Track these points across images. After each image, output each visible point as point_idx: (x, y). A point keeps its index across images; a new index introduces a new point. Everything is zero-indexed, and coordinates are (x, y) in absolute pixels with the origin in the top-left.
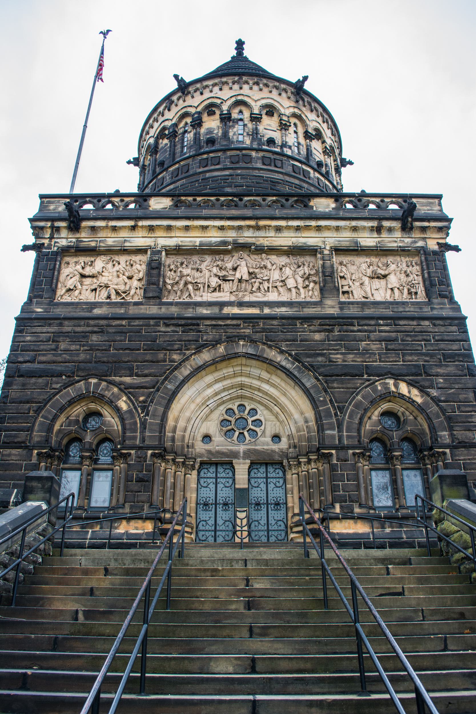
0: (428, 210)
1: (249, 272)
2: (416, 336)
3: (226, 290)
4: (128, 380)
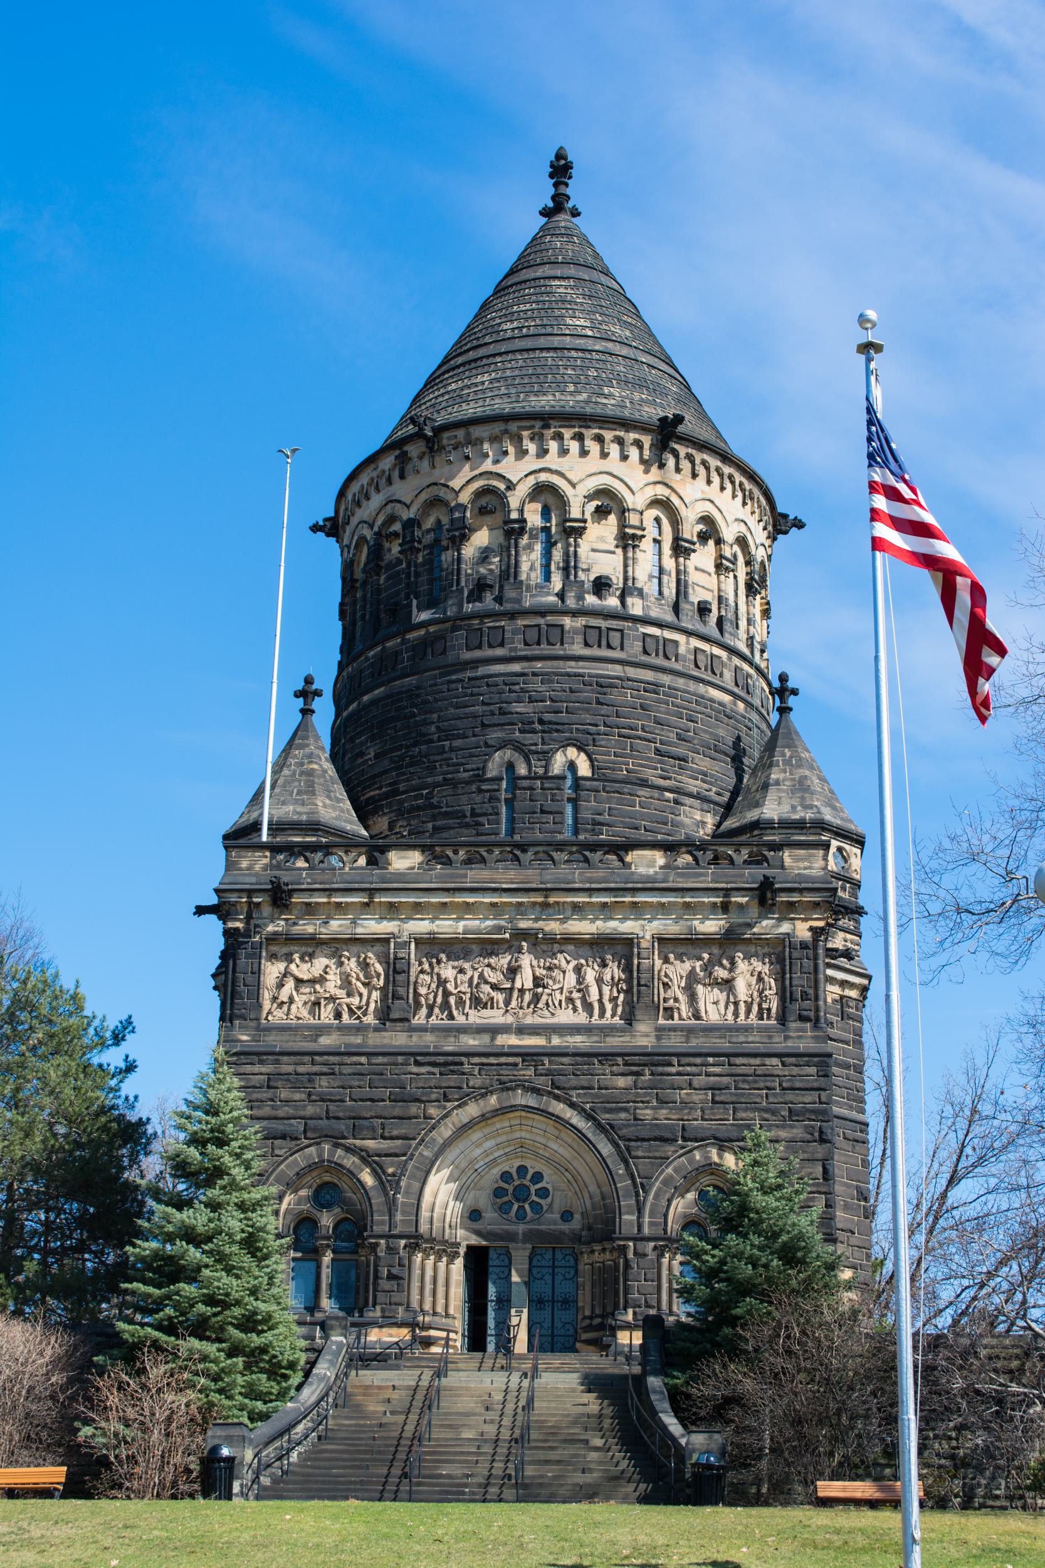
0: (805, 868)
2: (755, 1082)
4: (370, 1144)
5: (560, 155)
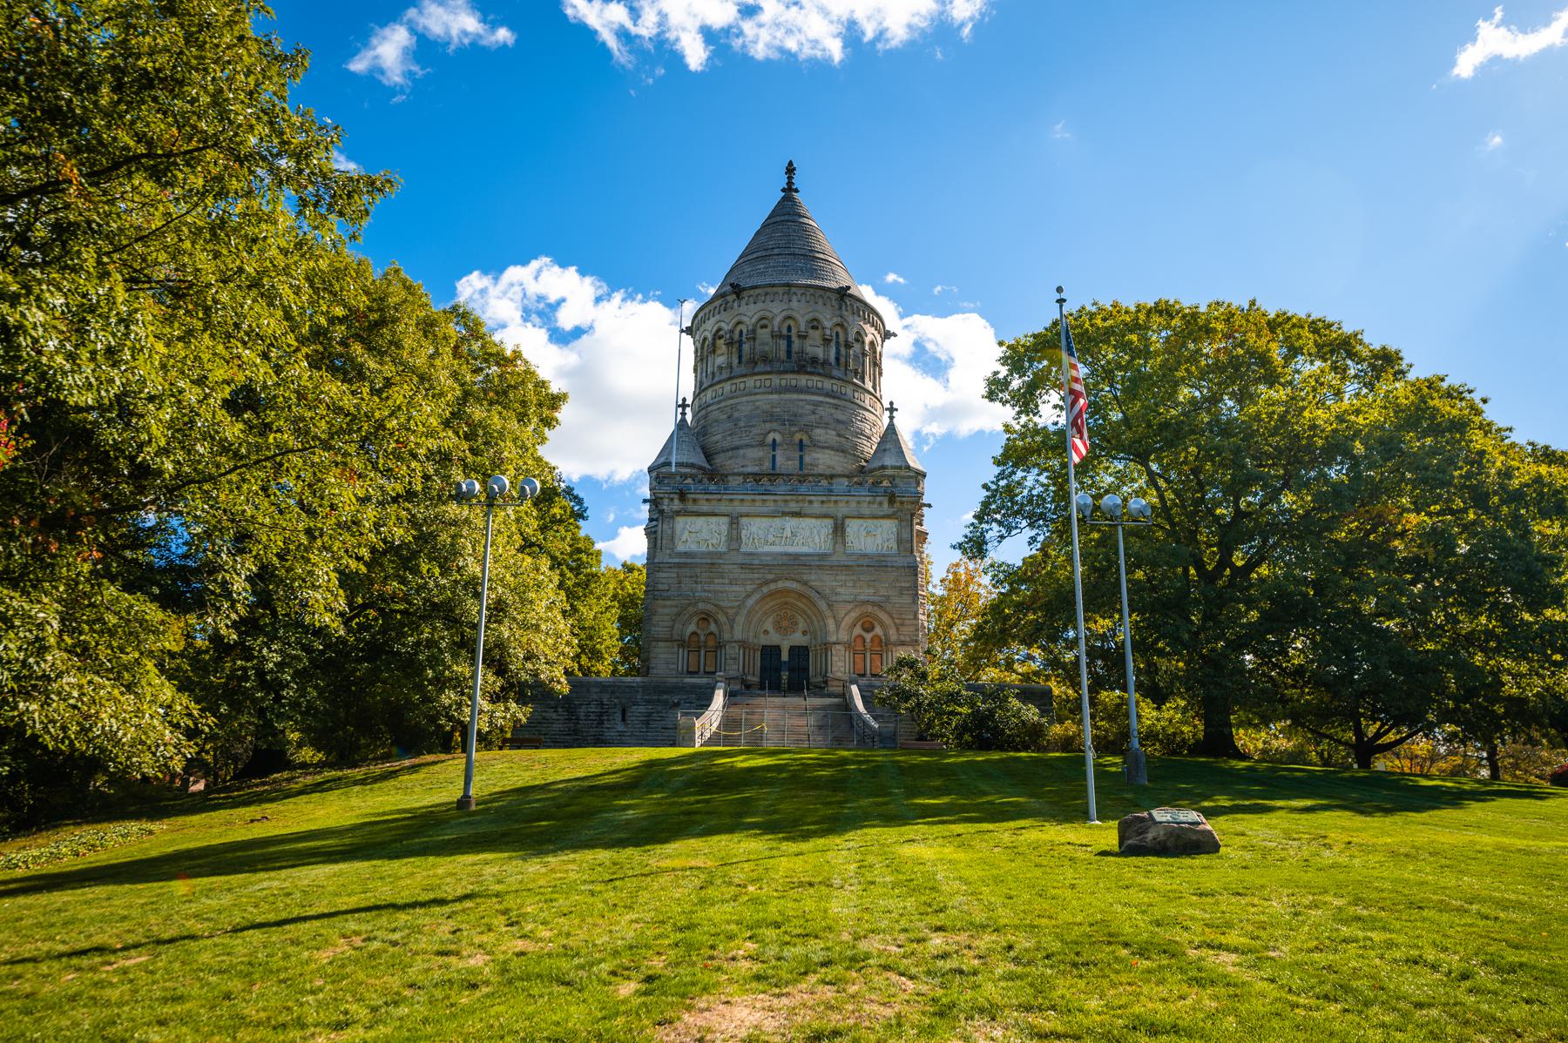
5: (791, 163)
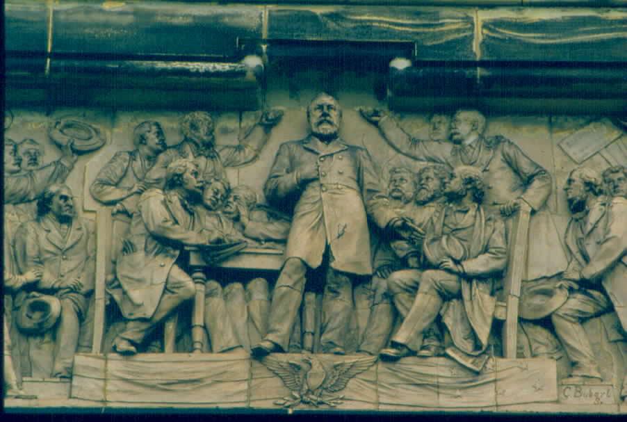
1: (372, 223)
3: (224, 337)
